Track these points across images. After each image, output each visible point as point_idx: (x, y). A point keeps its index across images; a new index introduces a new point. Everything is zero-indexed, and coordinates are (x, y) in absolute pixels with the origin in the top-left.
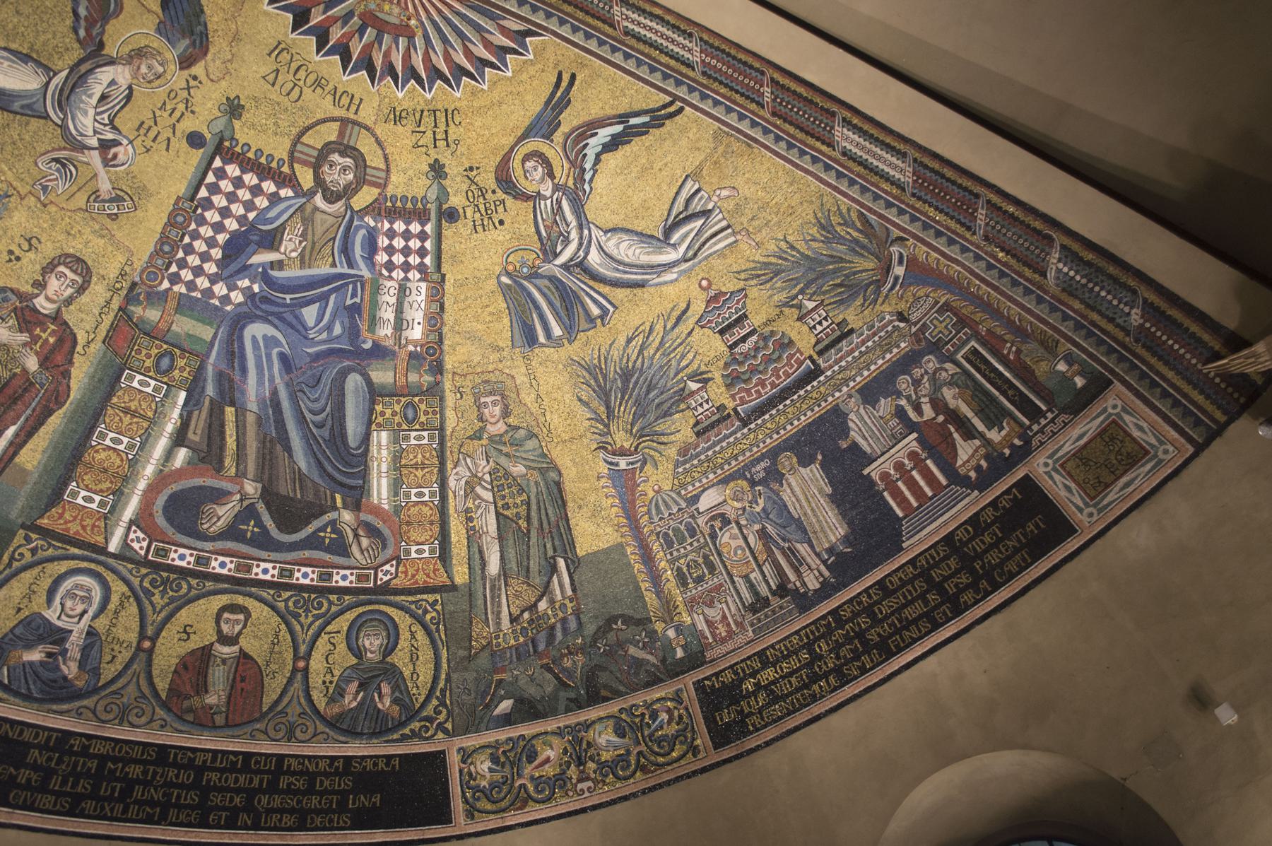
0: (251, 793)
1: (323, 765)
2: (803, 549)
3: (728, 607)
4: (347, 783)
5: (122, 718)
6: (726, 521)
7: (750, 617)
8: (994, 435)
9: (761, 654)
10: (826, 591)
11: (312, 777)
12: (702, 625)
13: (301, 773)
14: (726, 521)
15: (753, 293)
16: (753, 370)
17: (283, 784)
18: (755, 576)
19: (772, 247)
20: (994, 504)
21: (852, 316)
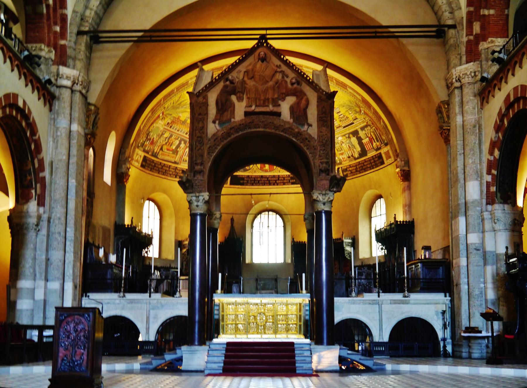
0: (276, 181)
1: (285, 176)
2: (355, 150)
3: (345, 156)
4: (289, 178)
5: (255, 172)
6: (343, 143)
7: (348, 159)
8: (377, 143)
9: (350, 165)
10: (358, 158)
11: (284, 178)
12: (341, 158)
13: (282, 177)
14: (343, 143)
15: (341, 108)
16: (343, 120)
17: (280, 179)
18: (348, 152)
19: (342, 102)
20: (377, 154)
21: (357, 115)
